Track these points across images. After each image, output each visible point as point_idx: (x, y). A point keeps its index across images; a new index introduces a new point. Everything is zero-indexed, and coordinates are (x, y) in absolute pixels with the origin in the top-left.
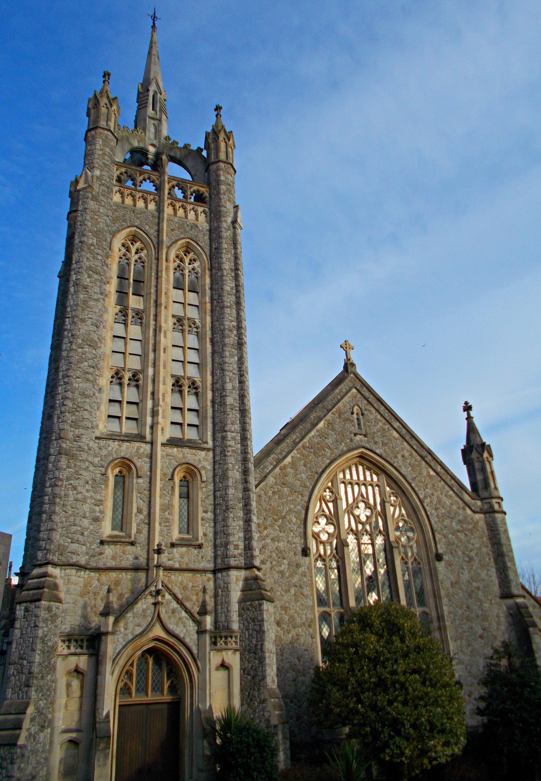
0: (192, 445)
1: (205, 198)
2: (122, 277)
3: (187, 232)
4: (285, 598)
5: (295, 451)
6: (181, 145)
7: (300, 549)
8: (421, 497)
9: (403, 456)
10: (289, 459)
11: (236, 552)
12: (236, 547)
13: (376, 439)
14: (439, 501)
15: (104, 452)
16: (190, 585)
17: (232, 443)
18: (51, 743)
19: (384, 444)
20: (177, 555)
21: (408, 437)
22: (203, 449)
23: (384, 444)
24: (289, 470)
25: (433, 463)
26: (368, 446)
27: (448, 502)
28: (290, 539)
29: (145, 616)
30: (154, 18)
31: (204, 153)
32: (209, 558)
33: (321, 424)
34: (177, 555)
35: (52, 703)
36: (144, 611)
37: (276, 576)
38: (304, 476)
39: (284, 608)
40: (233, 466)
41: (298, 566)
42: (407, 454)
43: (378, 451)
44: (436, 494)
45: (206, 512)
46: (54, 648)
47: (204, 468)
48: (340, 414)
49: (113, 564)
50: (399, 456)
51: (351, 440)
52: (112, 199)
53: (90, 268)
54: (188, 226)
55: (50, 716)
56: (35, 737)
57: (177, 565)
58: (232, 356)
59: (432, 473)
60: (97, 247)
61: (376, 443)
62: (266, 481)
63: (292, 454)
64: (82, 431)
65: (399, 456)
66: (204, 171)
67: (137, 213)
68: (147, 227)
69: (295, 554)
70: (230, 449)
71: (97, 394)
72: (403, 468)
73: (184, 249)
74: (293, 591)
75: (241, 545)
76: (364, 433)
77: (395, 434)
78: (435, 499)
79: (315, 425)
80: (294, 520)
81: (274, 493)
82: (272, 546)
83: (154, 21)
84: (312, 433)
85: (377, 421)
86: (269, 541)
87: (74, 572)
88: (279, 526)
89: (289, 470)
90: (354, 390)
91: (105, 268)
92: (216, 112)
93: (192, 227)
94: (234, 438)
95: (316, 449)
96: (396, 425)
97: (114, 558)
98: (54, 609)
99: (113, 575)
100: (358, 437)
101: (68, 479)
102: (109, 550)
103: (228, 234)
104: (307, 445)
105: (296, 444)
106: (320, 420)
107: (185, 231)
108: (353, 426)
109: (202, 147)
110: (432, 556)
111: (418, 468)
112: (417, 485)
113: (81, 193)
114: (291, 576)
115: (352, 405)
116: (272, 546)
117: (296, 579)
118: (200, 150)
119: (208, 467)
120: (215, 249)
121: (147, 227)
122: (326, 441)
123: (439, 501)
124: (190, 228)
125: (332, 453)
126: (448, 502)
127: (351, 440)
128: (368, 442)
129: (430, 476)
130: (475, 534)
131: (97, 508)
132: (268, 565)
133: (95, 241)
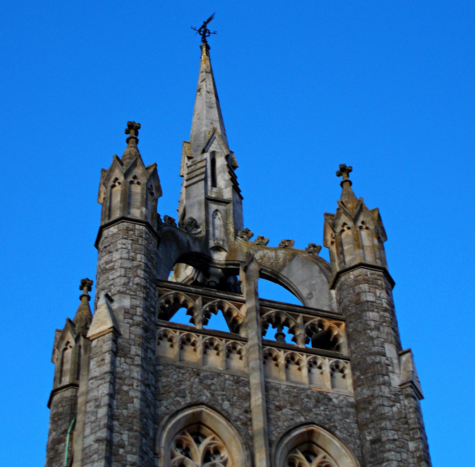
1: (336, 338)
3: (310, 410)
6: (274, 243)
30: (204, 32)
31: (324, 254)
52: (154, 352)
54: (308, 397)
60: (129, 448)
66: (327, 287)
67: (206, 377)
68: (226, 405)
73: (305, 447)
83: (204, 37)
92: (341, 179)
93: (318, 401)
103: (395, 409)
109: (319, 242)
113: (94, 343)
118: (314, 249)
120: (373, 442)
121: (226, 405)
124: (313, 401)
133: (125, 437)
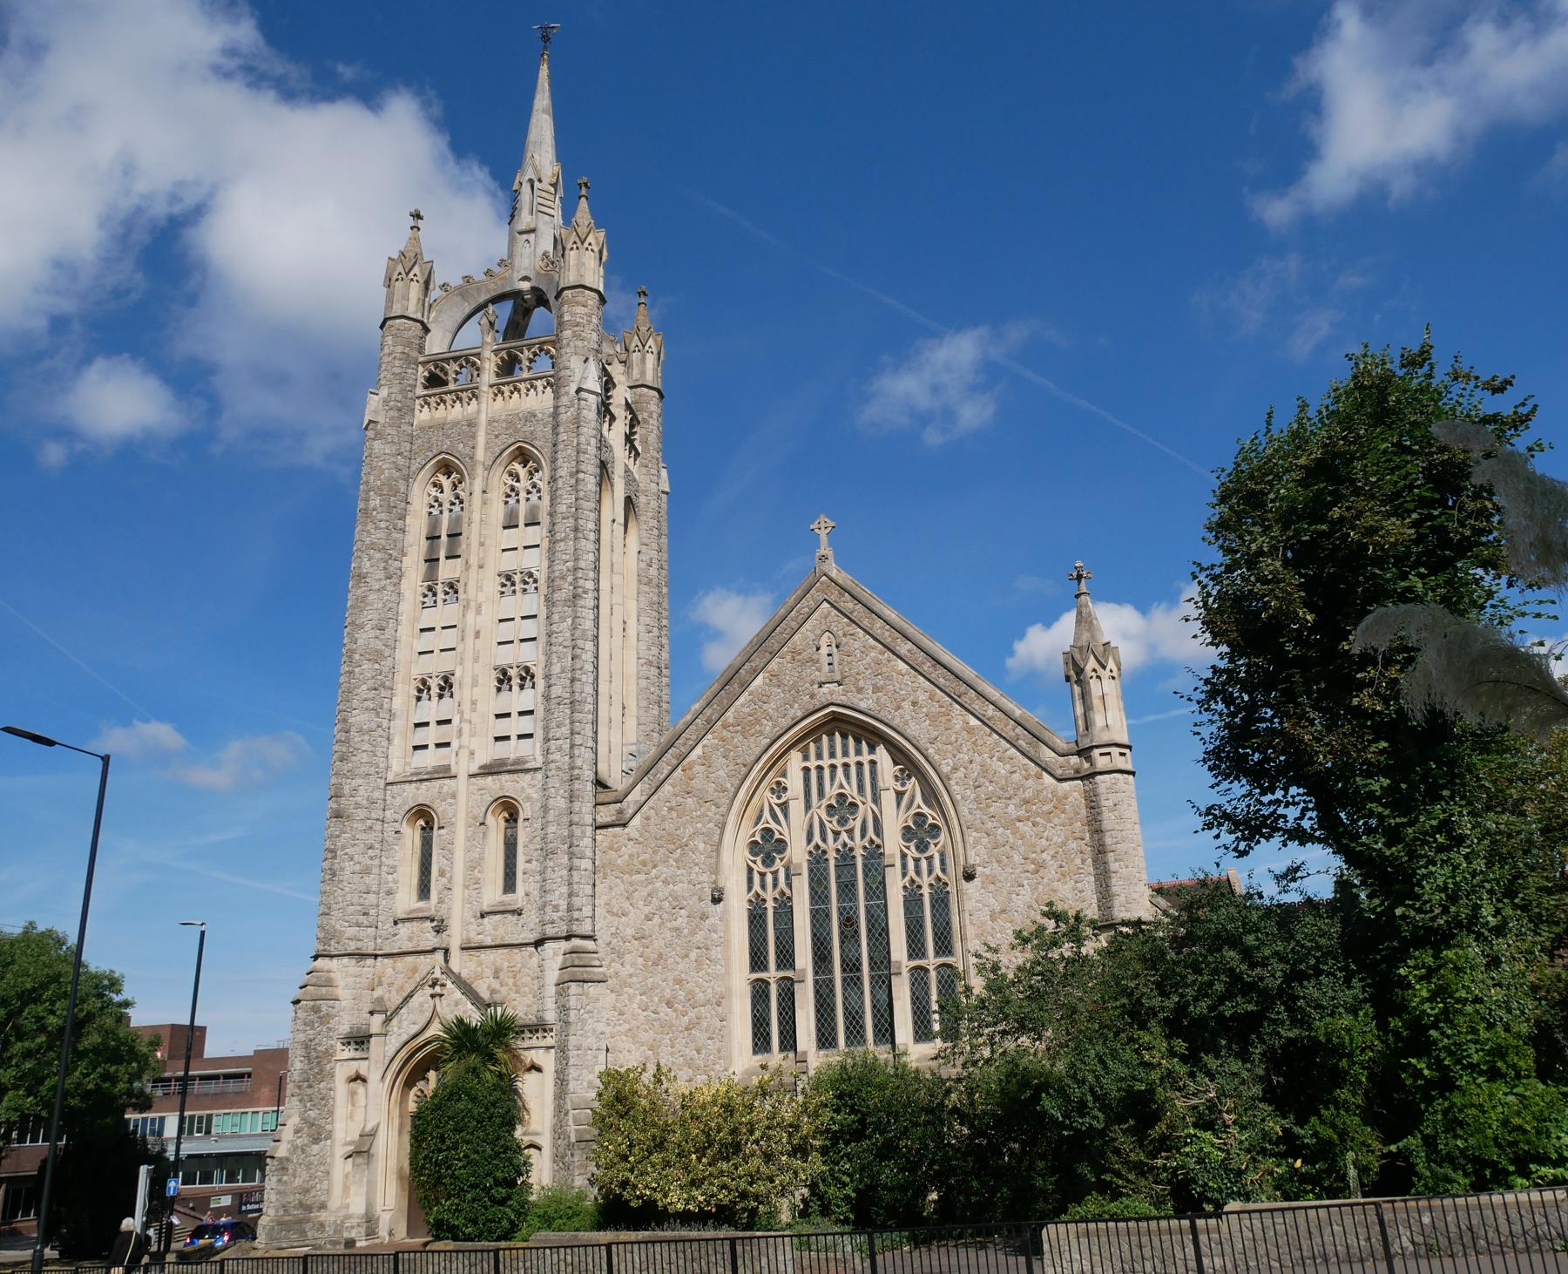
0: (517, 768)
2: (433, 538)
4: (680, 967)
5: (709, 736)
7: (708, 891)
8: (945, 769)
9: (914, 704)
10: (698, 751)
11: (555, 916)
12: (556, 908)
13: (861, 684)
14: (985, 770)
15: (399, 800)
16: (506, 964)
17: (556, 756)
18: (332, 1155)
19: (876, 689)
20: (488, 927)
21: (927, 667)
22: (527, 771)
23: (876, 689)
24: (697, 768)
25: (977, 705)
26: (843, 699)
27: (1002, 770)
28: (693, 876)
29: (422, 1012)
32: (532, 926)
33: (759, 681)
34: (488, 927)
35: (331, 1113)
36: (421, 1005)
37: (668, 934)
38: (721, 773)
39: (679, 982)
40: (557, 790)
41: (704, 917)
42: (922, 697)
43: (863, 705)
44: (978, 759)
45: (529, 861)
46: (329, 1054)
47: (528, 798)
48: (795, 652)
49: (408, 947)
50: (906, 705)
51: (812, 696)
53: (373, 546)
55: (328, 1127)
56: (303, 1151)
57: (489, 942)
58: (563, 619)
59: (974, 722)
61: (860, 690)
62: (659, 793)
63: (704, 742)
64: (360, 781)
65: (906, 705)
69: (700, 900)
70: (552, 766)
71: (385, 725)
72: (912, 724)
74: (693, 955)
75: (563, 905)
76: (838, 678)
77: (902, 666)
78: (976, 767)
79: (745, 686)
80: (701, 846)
81: (671, 809)
82: (663, 891)
84: (742, 699)
85: (865, 650)
86: (659, 884)
87: (353, 961)
88: (676, 861)
89: (697, 768)
90: (825, 605)
91: (395, 535)
94: (560, 749)
95: (746, 726)
96: (904, 648)
97: (410, 939)
98: (324, 1008)
99: (409, 959)
100: (826, 688)
101: (344, 847)
102: (404, 929)
104: (731, 720)
105: (711, 724)
106: (755, 673)
107: (517, 431)
108: (819, 670)
110: (960, 870)
111: (943, 719)
112: (938, 751)
114: (693, 933)
115: (818, 632)
116: (663, 891)
117: (699, 937)
119: (535, 796)
122: (765, 707)
123: (985, 770)
125: (774, 726)
126: (1002, 770)
127: (812, 696)
128: (845, 693)
129: (970, 731)
130: (1056, 821)
131: (390, 877)
132: (656, 920)
